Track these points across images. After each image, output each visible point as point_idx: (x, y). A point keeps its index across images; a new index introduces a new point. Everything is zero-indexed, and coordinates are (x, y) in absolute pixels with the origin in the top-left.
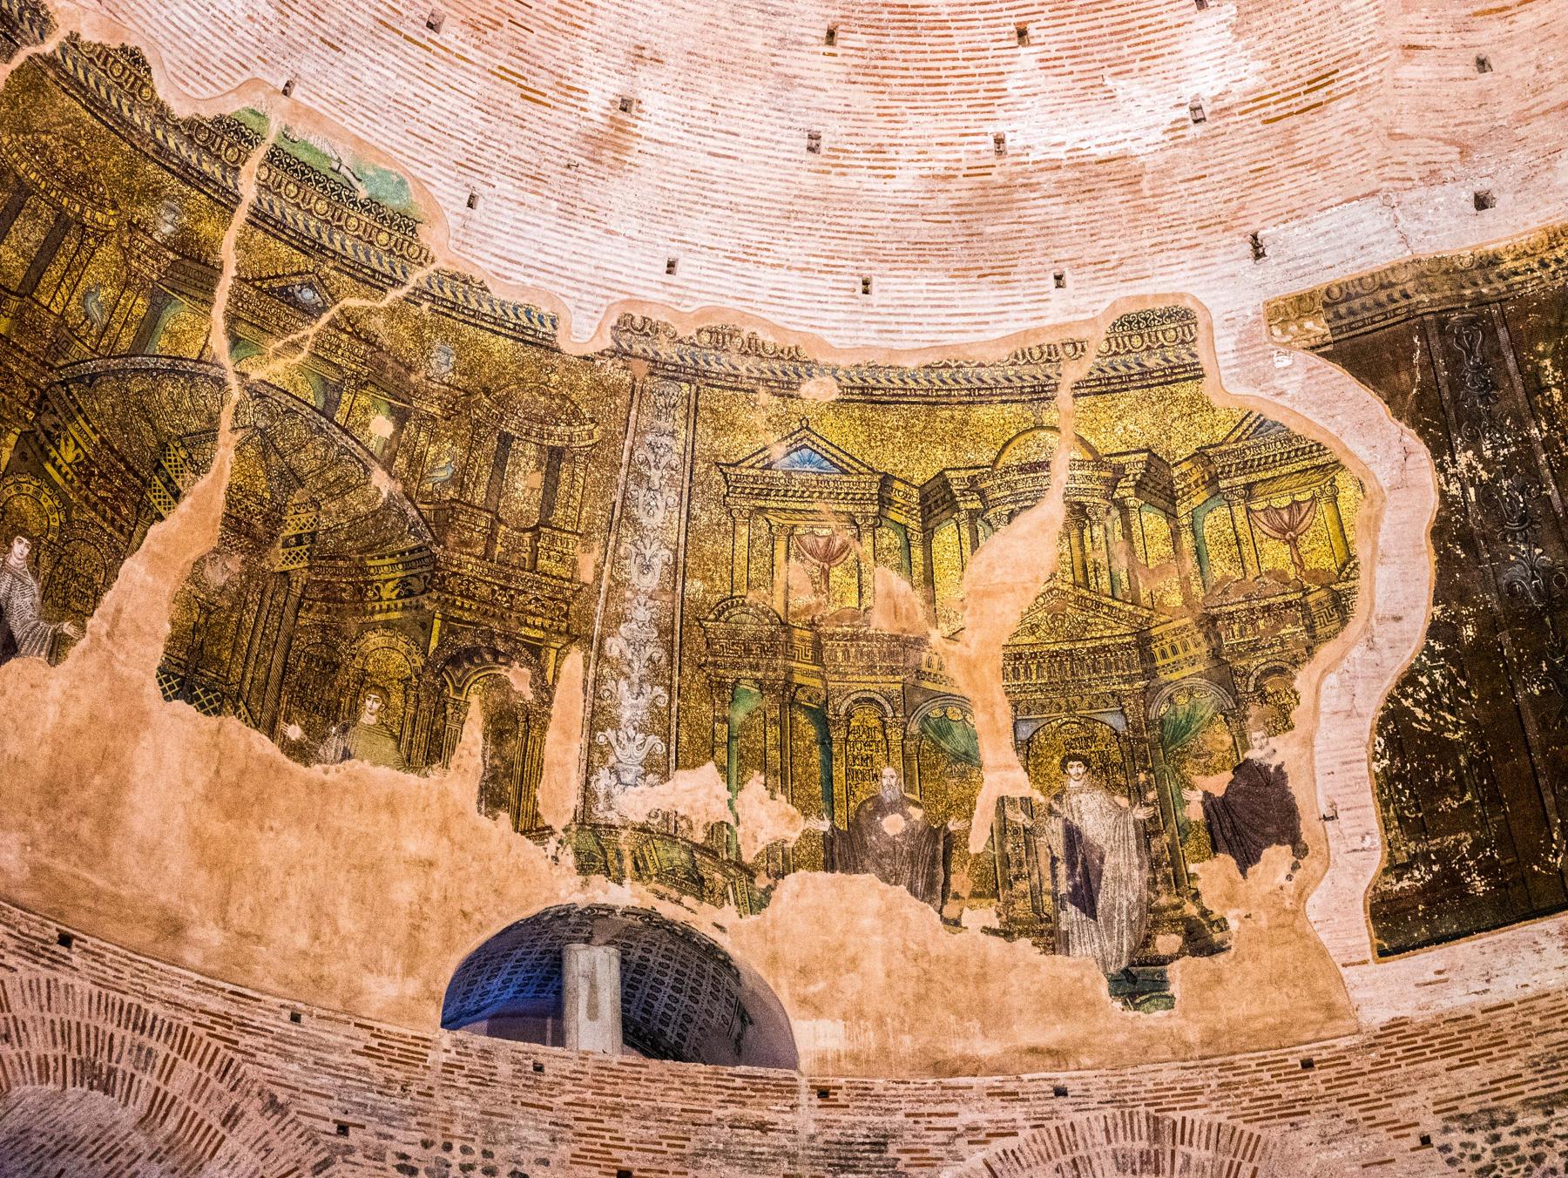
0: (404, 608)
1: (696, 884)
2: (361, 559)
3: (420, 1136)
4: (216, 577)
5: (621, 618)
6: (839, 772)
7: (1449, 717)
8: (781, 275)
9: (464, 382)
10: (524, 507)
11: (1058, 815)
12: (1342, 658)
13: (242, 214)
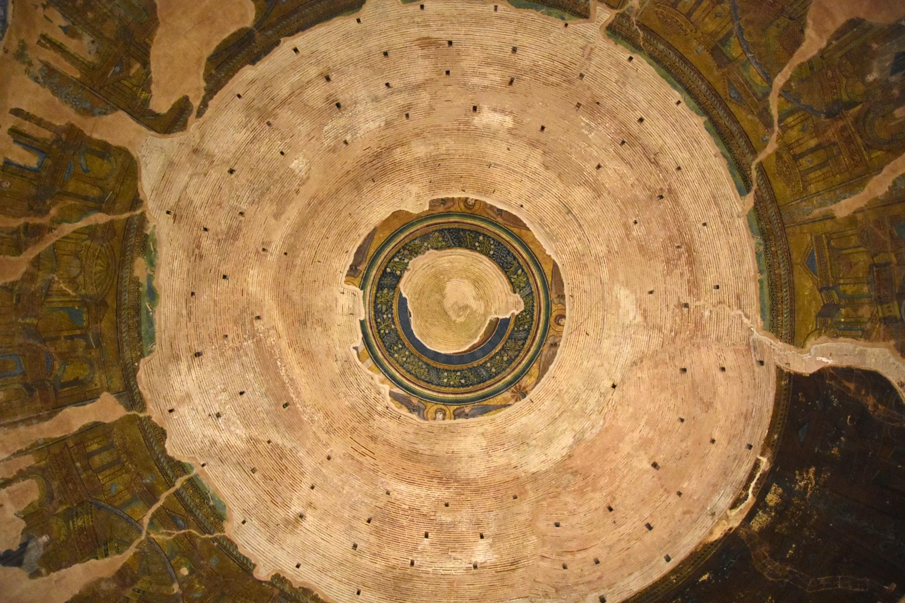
4: (104, 586)
8: (332, 581)
13: (172, 490)
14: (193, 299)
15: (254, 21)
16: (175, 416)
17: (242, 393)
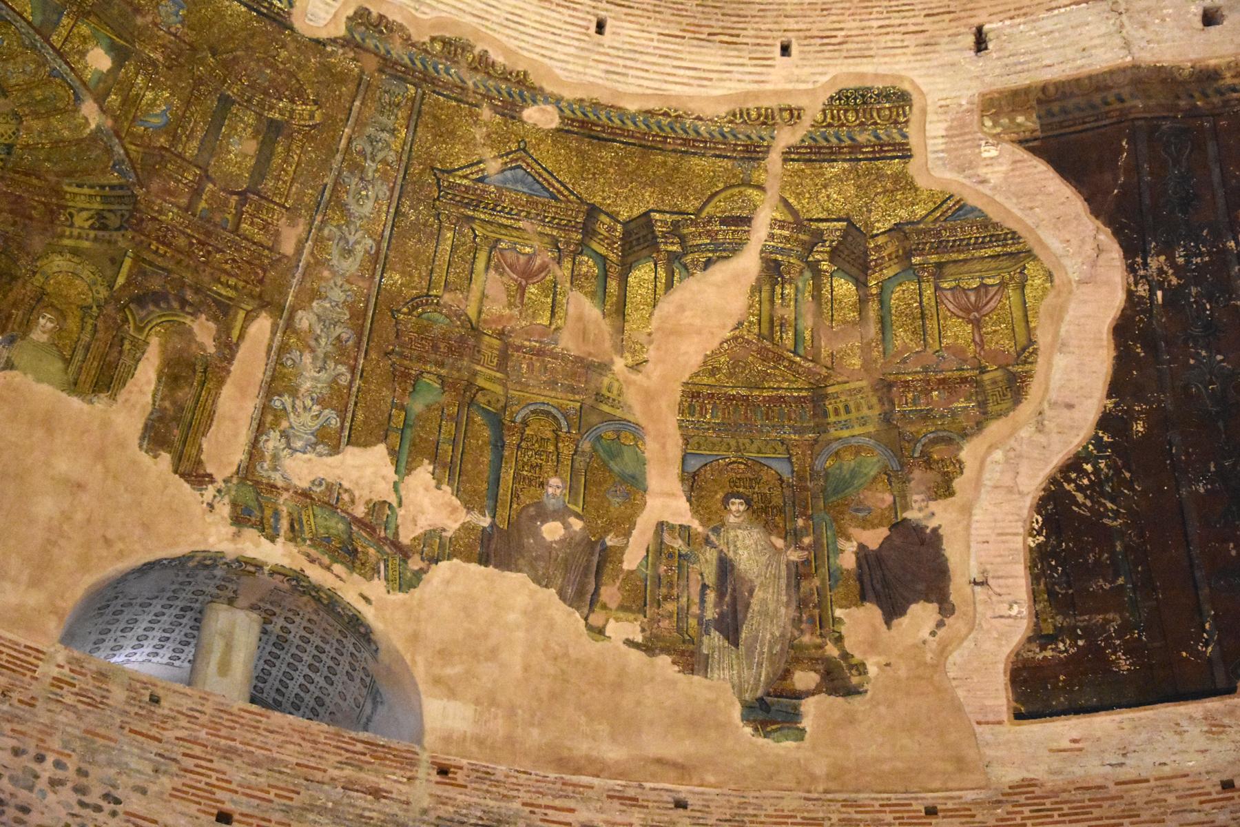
0: (96, 239)
1: (349, 555)
2: (58, 183)
3: (13, 742)
5: (316, 295)
6: (508, 475)
7: (1109, 505)
9: (191, 36)
10: (235, 170)
12: (1011, 435)
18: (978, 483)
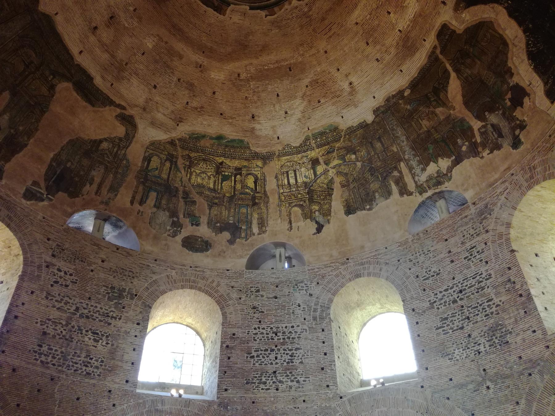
1: (439, 183)
3: (411, 254)
5: (405, 152)
6: (451, 147)
11: (488, 124)
14: (224, 115)
15: (68, 82)
16: (281, 137)
17: (278, 95)
18: (516, 67)
